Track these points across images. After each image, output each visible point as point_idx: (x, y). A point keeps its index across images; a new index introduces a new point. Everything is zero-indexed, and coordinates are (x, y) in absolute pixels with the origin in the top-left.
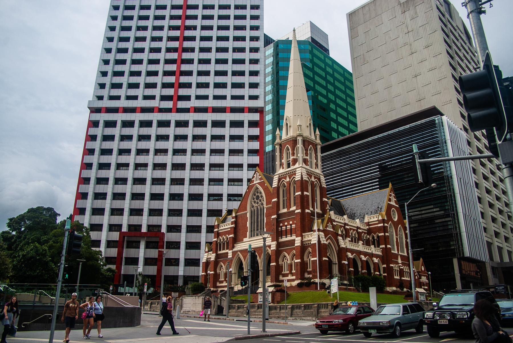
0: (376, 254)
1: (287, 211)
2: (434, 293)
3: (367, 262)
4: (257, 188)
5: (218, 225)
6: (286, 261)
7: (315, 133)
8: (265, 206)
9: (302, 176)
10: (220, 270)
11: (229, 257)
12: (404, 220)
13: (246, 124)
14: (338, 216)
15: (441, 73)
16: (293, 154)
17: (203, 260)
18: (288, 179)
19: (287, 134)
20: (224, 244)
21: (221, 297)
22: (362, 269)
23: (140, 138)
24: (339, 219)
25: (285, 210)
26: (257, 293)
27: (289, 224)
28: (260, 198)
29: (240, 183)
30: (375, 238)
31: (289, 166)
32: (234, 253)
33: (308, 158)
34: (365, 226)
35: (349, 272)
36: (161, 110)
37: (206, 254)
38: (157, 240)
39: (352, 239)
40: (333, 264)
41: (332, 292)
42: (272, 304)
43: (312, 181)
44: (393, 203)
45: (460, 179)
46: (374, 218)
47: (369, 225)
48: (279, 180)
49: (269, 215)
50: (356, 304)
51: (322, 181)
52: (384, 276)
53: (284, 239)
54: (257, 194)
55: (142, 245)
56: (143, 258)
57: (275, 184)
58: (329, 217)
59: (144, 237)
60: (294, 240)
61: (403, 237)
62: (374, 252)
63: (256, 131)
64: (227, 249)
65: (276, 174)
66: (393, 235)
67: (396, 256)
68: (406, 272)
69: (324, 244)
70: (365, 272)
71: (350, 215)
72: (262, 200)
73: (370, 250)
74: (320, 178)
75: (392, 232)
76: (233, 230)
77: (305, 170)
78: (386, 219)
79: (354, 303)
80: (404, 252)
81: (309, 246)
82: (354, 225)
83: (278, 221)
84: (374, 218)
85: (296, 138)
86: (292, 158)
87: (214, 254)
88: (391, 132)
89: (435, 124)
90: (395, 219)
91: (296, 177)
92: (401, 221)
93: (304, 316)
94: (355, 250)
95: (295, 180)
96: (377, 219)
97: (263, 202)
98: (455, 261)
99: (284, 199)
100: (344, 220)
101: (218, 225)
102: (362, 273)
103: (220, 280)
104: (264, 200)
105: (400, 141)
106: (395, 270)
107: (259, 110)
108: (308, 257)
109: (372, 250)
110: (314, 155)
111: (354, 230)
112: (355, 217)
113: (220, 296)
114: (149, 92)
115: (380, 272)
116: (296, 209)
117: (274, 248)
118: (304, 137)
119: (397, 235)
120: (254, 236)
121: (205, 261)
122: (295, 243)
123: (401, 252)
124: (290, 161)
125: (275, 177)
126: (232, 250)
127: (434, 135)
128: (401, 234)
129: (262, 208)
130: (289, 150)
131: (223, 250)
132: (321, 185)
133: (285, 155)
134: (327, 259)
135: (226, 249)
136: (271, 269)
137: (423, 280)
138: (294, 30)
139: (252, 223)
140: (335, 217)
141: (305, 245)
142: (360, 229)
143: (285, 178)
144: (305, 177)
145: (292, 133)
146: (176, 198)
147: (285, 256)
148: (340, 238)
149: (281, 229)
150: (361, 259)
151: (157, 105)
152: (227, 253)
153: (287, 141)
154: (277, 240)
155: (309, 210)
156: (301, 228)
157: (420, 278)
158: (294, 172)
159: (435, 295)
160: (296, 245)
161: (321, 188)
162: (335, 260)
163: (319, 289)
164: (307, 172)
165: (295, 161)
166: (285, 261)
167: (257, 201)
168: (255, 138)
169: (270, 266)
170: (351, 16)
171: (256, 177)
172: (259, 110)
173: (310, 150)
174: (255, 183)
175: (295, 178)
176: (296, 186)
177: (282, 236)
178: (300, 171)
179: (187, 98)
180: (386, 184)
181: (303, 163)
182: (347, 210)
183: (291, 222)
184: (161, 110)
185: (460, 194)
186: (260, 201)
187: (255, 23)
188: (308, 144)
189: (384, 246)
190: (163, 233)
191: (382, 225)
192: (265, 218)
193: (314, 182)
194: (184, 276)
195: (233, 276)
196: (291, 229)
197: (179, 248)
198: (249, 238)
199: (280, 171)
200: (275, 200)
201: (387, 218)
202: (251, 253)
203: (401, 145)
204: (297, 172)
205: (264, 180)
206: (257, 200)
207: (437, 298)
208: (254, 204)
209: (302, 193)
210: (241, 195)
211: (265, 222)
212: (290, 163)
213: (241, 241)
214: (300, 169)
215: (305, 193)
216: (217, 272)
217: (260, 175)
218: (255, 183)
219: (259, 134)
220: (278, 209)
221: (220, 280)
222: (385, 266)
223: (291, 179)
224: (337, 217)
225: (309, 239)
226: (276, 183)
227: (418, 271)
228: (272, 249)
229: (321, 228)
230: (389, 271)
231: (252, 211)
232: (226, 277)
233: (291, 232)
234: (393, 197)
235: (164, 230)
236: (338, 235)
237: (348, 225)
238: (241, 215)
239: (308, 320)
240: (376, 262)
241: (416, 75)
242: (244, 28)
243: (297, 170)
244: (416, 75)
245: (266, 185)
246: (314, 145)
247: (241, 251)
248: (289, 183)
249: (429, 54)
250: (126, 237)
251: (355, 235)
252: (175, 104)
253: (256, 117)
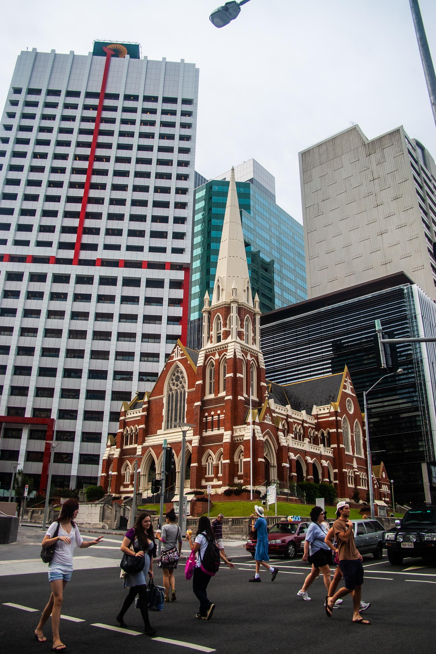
0: (326, 456)
1: (214, 397)
2: (397, 507)
3: (314, 465)
4: (178, 367)
5: (126, 412)
6: (211, 461)
7: (253, 298)
8: (187, 390)
9: (235, 353)
10: (126, 470)
11: (138, 454)
12: (362, 413)
13: (167, 284)
14: (279, 406)
15: (412, 232)
16: (225, 325)
17: (104, 456)
18: (217, 357)
19: (219, 300)
20: (132, 436)
21: (125, 506)
22: (308, 474)
23: (30, 295)
24: (280, 410)
25: (212, 396)
26: (173, 502)
27: (216, 414)
28: (181, 379)
29: (155, 359)
30: (325, 435)
31: (219, 340)
32: (144, 449)
33: (244, 330)
34: (313, 419)
35: (291, 478)
36: (59, 261)
37: (109, 449)
38: (45, 428)
39: (296, 435)
40: (271, 467)
41: (269, 503)
42: (191, 516)
43: (247, 360)
44: (348, 391)
45: (433, 363)
46: (324, 409)
47: (318, 418)
48: (206, 357)
49: (191, 402)
50: (298, 519)
51: (260, 360)
52: (335, 484)
53: (209, 433)
54: (176, 374)
55: (25, 434)
56: (25, 451)
57: (200, 362)
58: (268, 406)
59: (28, 424)
60: (222, 435)
61: (359, 435)
62: (323, 453)
63: (179, 294)
64: (136, 443)
65: (202, 349)
66: (347, 432)
67: (351, 459)
68: (363, 479)
69: (260, 440)
70: (311, 478)
71: (294, 405)
72: (183, 381)
73: (319, 450)
74: (258, 357)
75: (347, 428)
76: (144, 418)
77: (239, 345)
78: (339, 411)
79: (296, 519)
80: (360, 454)
81: (241, 443)
82: (298, 417)
83: (202, 410)
84: (324, 409)
85: (230, 305)
86: (223, 329)
87: (119, 450)
88: (349, 302)
89: (403, 294)
90: (350, 412)
91: (228, 354)
92: (358, 414)
93: (231, 534)
94: (299, 449)
95: (226, 358)
96: (328, 411)
97: (184, 384)
98: (424, 467)
99: (211, 381)
100: (286, 410)
101: (126, 412)
102: (307, 480)
103: (125, 483)
104: (185, 382)
105: (360, 314)
106: (349, 476)
107: (184, 266)
108: (240, 457)
109: (321, 449)
110: (251, 327)
111: (299, 424)
112: (301, 407)
113: (123, 504)
114: (45, 237)
115: (329, 479)
116: (226, 396)
117: (196, 444)
118: (240, 303)
119: (352, 432)
120: (171, 428)
121: (106, 458)
122: (223, 439)
123: (357, 454)
124: (220, 333)
125: (200, 353)
126: (142, 444)
127: (402, 308)
128: (357, 430)
129: (183, 392)
130: (220, 319)
131: (130, 444)
132: (259, 366)
133: (214, 325)
134: (263, 460)
135: (134, 444)
136: (191, 471)
137: (384, 490)
138: (233, 169)
139: (169, 410)
140: (276, 406)
141: (235, 441)
142: (306, 422)
143: (214, 355)
144: (239, 354)
145: (224, 299)
146: (73, 374)
147: (210, 455)
148: (280, 434)
149: (206, 420)
150: (306, 461)
151: (54, 254)
152: (136, 449)
153: (219, 309)
154: (201, 434)
155: (242, 396)
156: (231, 420)
157: (380, 487)
158: (226, 347)
159: (399, 510)
160: (224, 441)
161: (259, 369)
162: (274, 461)
163: (251, 499)
164: (241, 348)
165: (227, 334)
166: (209, 461)
167: (176, 383)
168: (177, 302)
169: (190, 467)
170: (304, 156)
171: (176, 352)
172: (184, 266)
173: (246, 321)
174: (174, 359)
175: (226, 355)
176: (227, 365)
177: (206, 429)
178: (233, 347)
179: (93, 247)
180: (341, 367)
181: (237, 336)
182: (290, 399)
183: (219, 412)
184: (59, 261)
185: (432, 383)
186: (181, 383)
187: (184, 157)
188: (245, 313)
189: (335, 446)
190: (53, 419)
191: (334, 418)
192: (186, 405)
193: (250, 361)
194: (78, 478)
195: (142, 479)
196: (219, 420)
197: (73, 440)
198: (165, 430)
199: (207, 346)
200: (200, 382)
201: (341, 409)
202: (167, 450)
203: (360, 318)
204: (229, 348)
205: (187, 356)
206: (177, 381)
207: (400, 513)
208: (172, 387)
209: (235, 375)
210: (156, 374)
211: (186, 410)
212: (221, 336)
213: (154, 433)
214: (233, 344)
215: (239, 375)
216: (122, 473)
217: (181, 350)
218: (174, 359)
219: (182, 297)
220: (203, 394)
221: (125, 483)
222: (336, 471)
223: (221, 356)
224: (278, 407)
225: (241, 434)
226: (202, 361)
227: (377, 478)
228: (193, 445)
229: (257, 420)
230: (341, 476)
231: (169, 395)
232: (132, 480)
233: (218, 424)
234: (349, 384)
235: (54, 415)
236: (278, 429)
237: (291, 418)
238: (156, 399)
239: (236, 539)
240: (325, 466)
241: (381, 232)
242: (170, 163)
243: (229, 345)
244: (381, 232)
245: (189, 363)
246: (252, 315)
247: (154, 447)
248: (218, 362)
249: (398, 208)
250: (3, 424)
251: (299, 430)
252: (77, 254)
253: (180, 275)
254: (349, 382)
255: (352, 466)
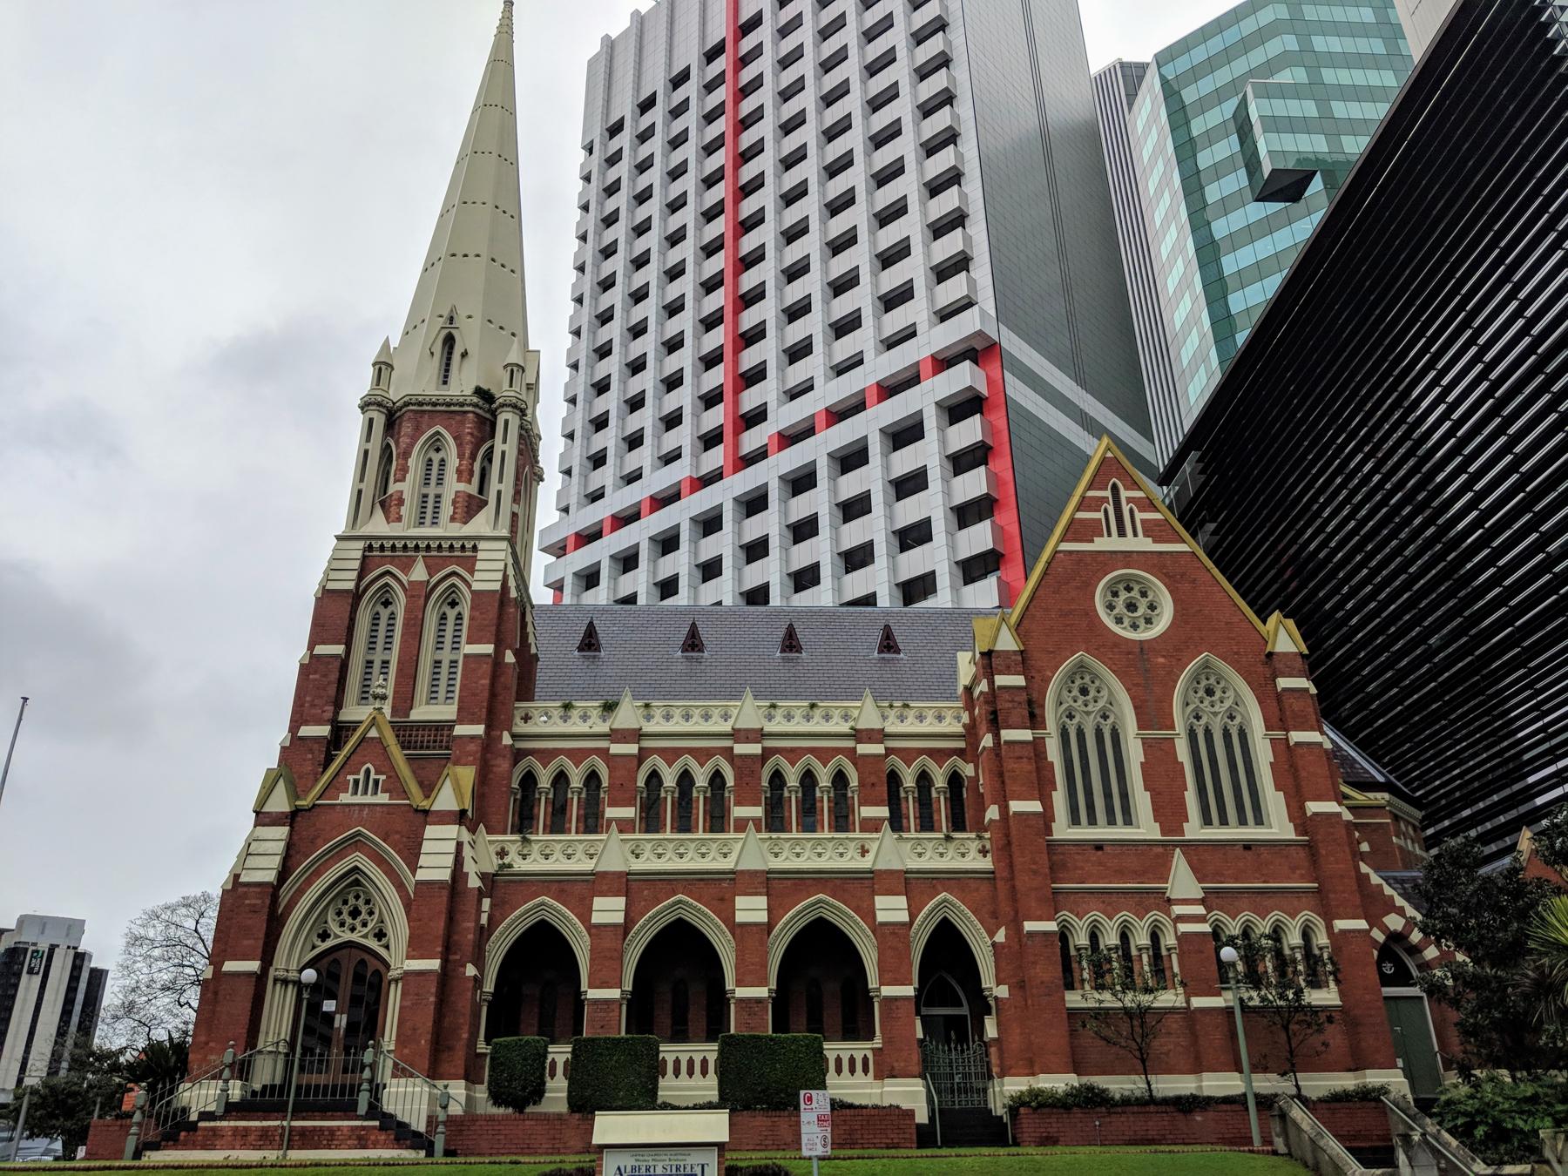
43: (410, 583)
110: (453, 462)
254: (1129, 500)
255: (1162, 892)
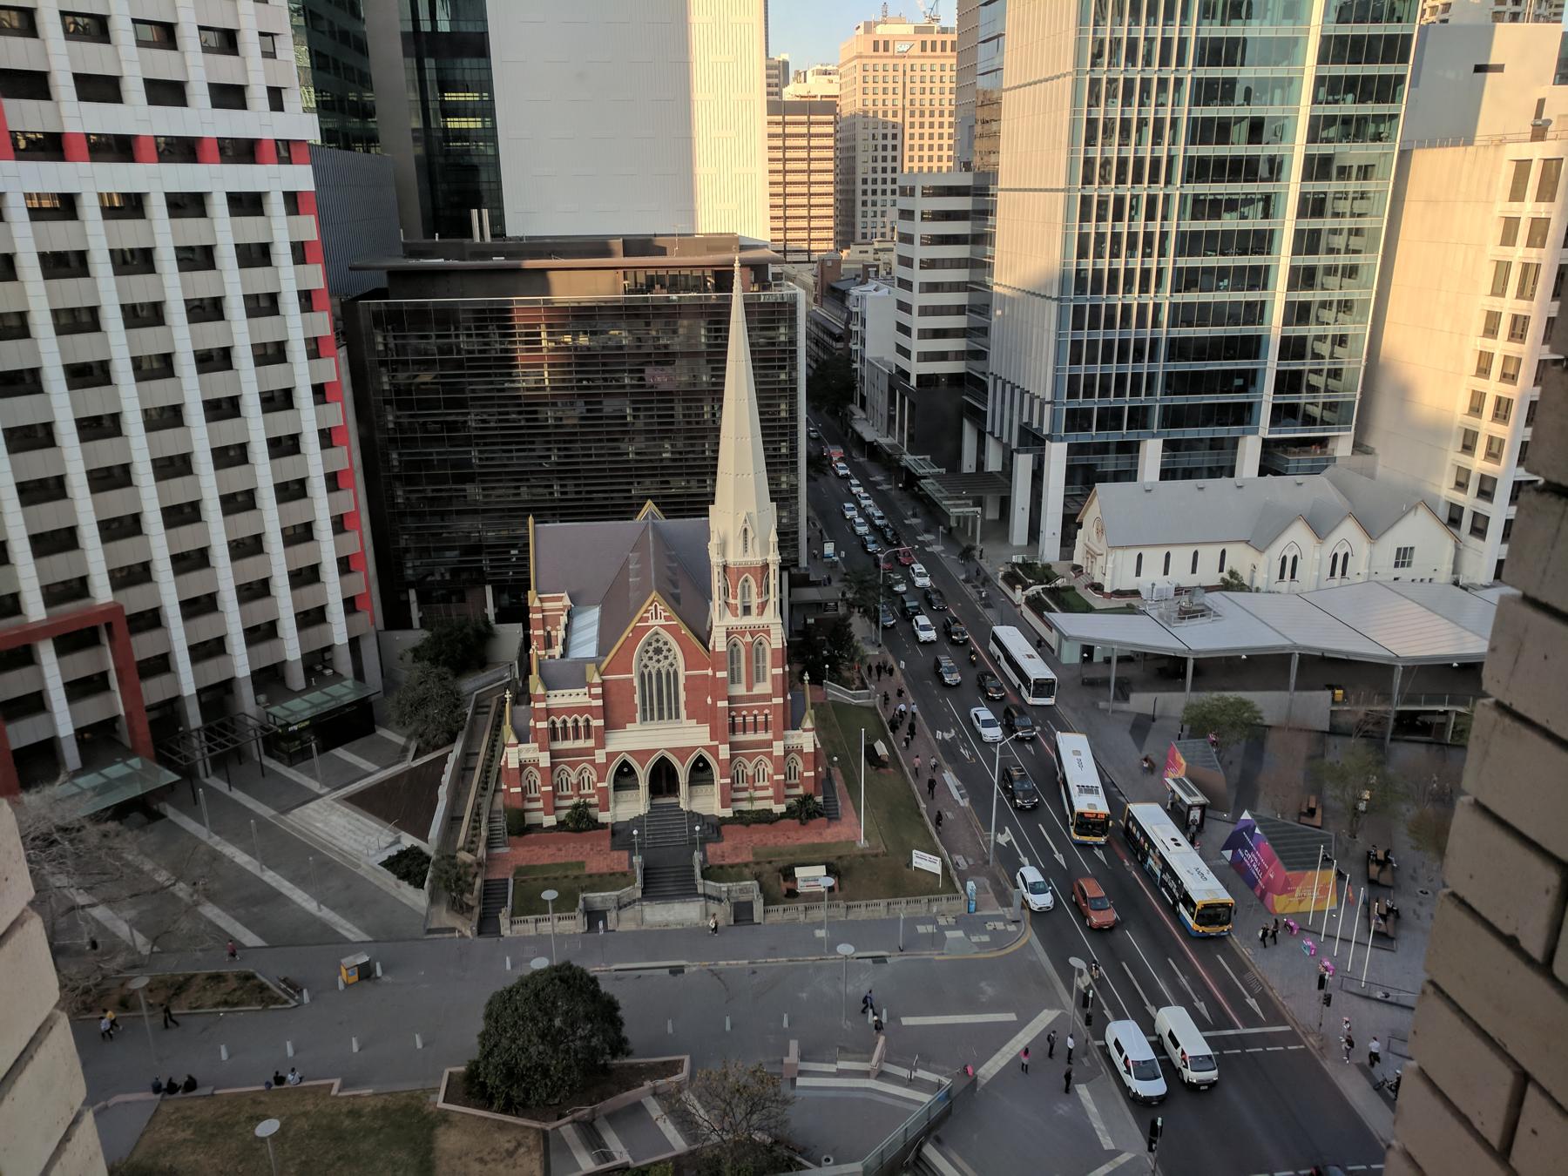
18: (748, 639)
32: (611, 756)
120: (652, 719)
143: (743, 634)
208: (649, 663)
238: (616, 680)
